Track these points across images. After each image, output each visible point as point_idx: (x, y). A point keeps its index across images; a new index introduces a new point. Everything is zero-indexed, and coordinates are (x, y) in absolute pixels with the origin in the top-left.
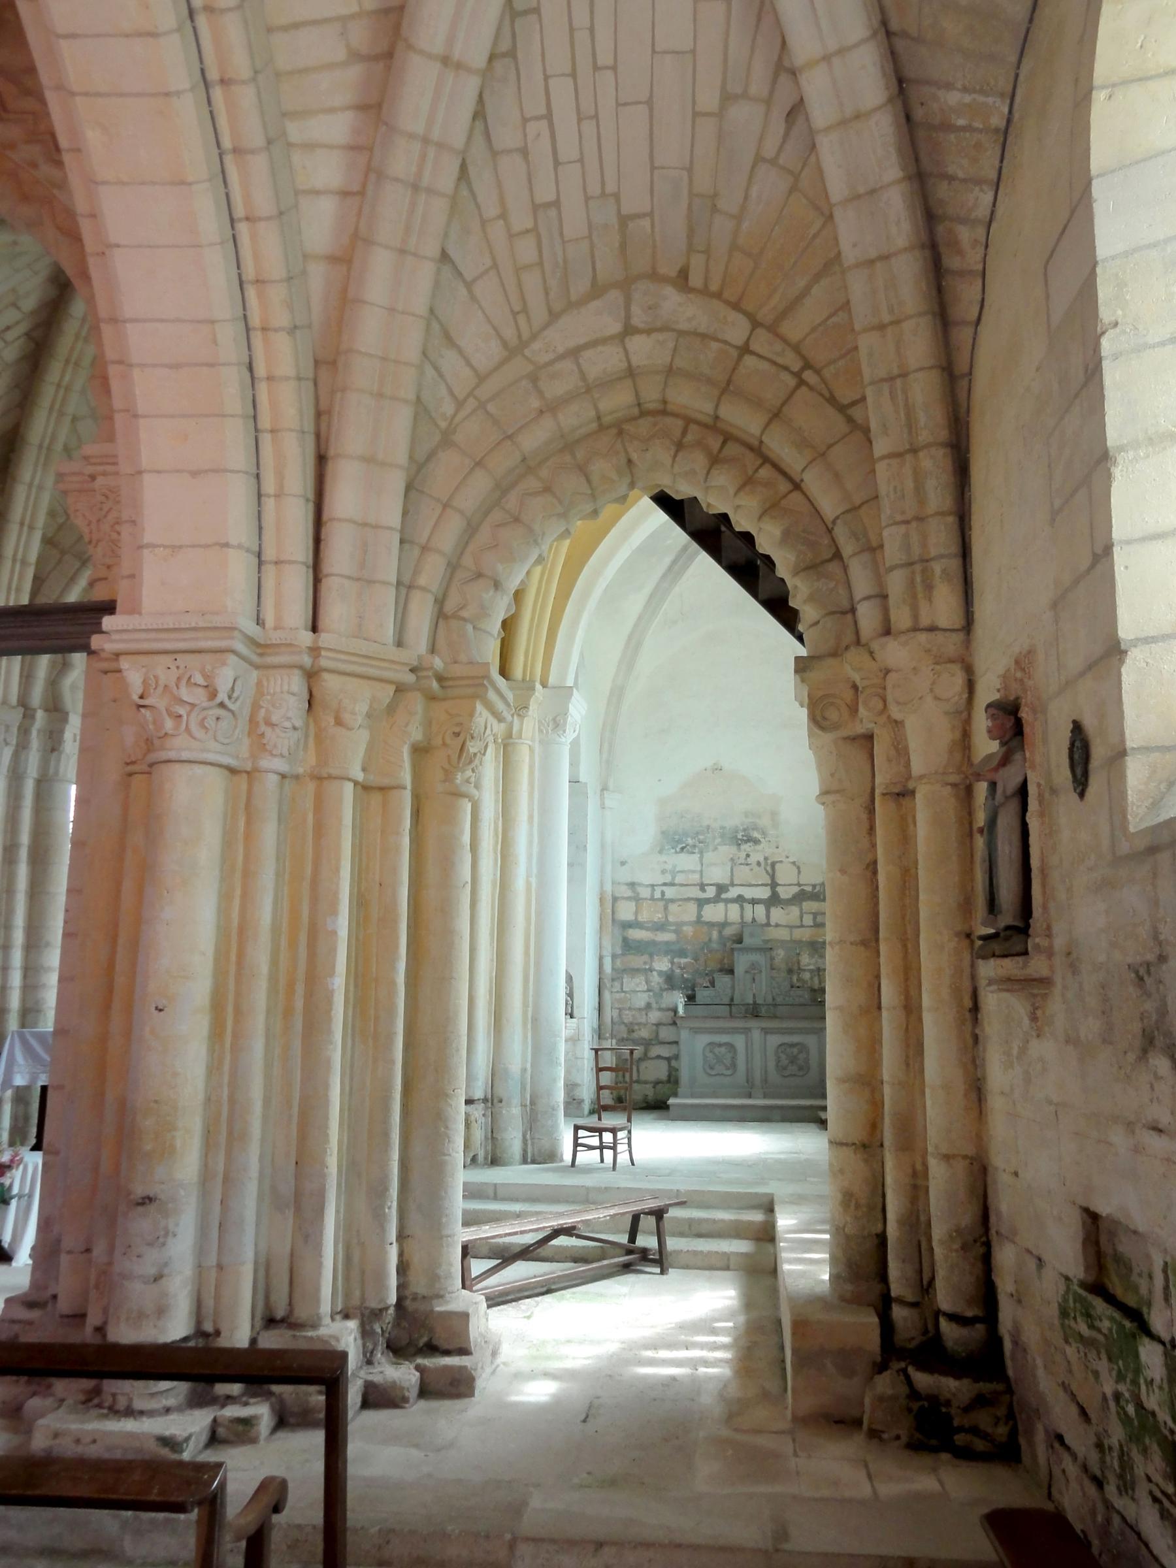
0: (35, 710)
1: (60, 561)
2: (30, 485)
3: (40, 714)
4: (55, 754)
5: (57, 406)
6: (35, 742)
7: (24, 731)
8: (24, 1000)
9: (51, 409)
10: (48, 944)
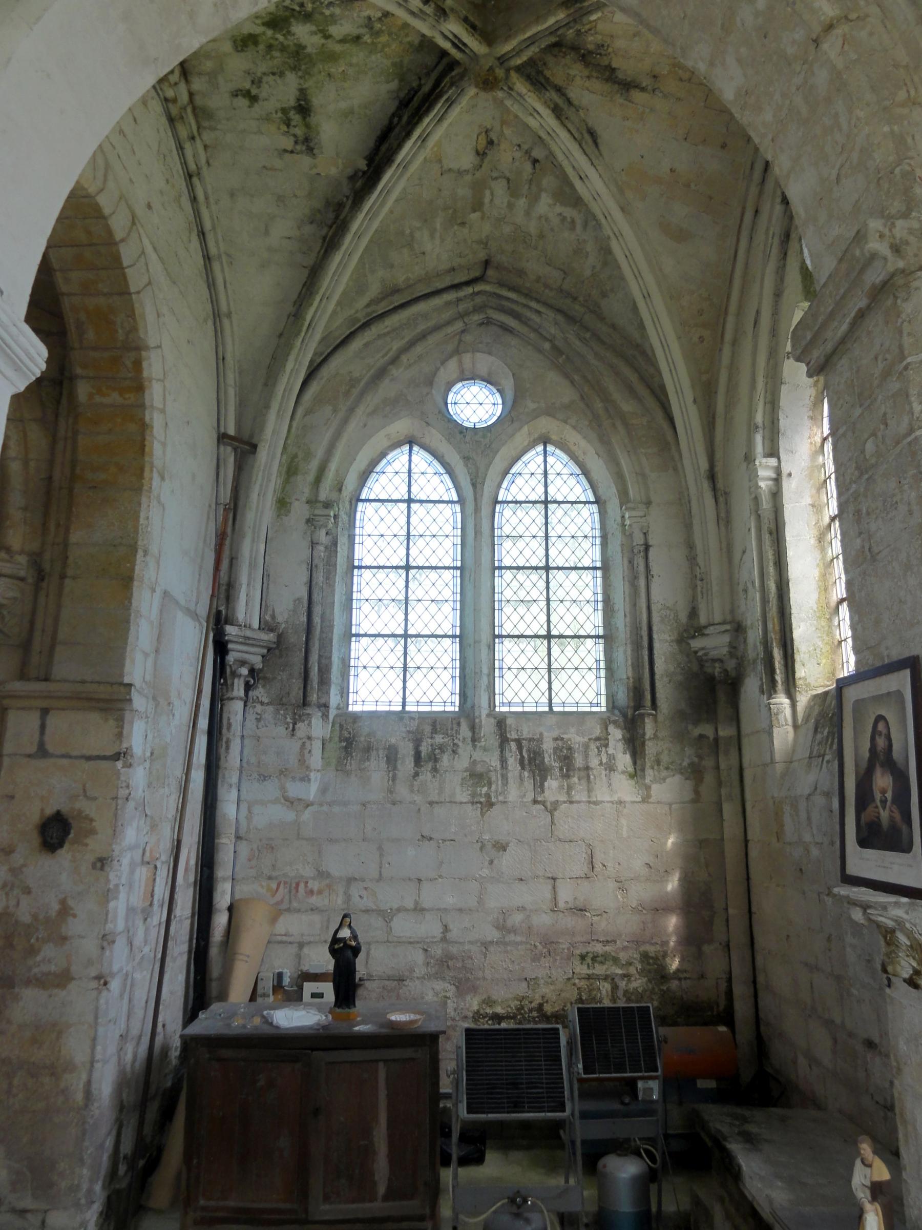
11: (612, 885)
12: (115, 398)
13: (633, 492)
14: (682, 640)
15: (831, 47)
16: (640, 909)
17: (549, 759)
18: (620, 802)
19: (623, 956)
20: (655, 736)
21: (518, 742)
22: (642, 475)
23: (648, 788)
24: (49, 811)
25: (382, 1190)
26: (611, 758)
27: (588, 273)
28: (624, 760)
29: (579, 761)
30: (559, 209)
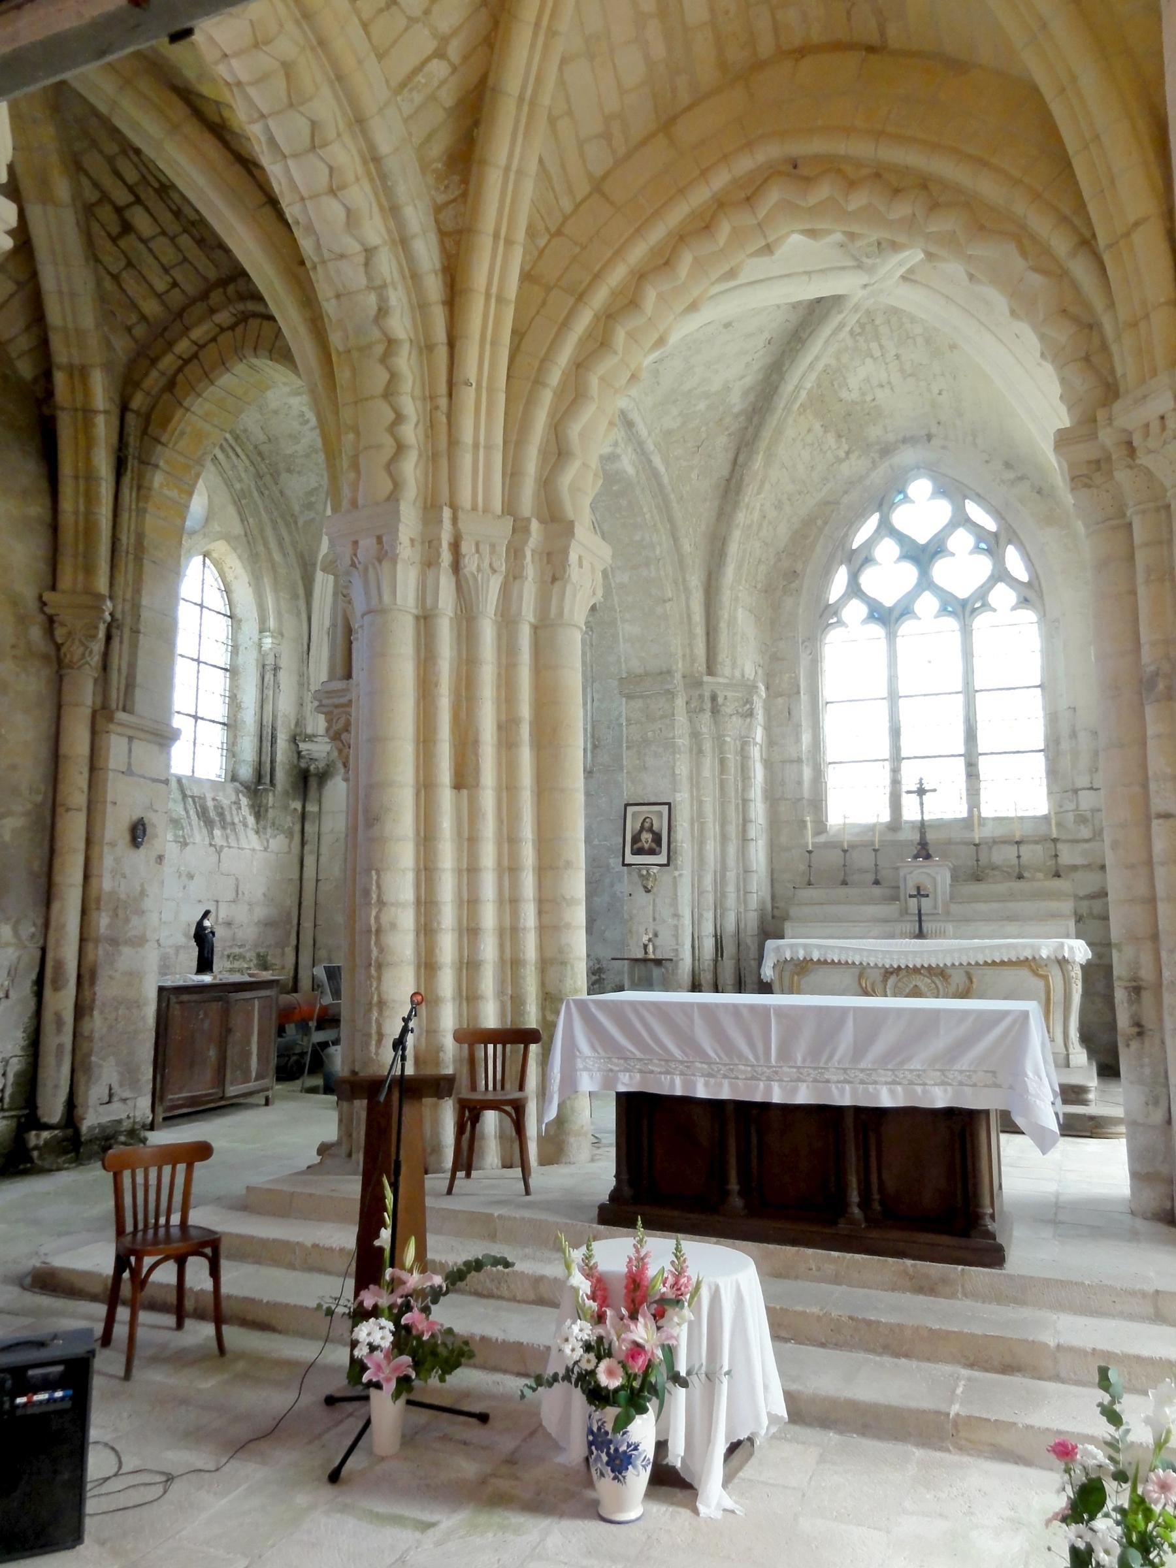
0: (528, 520)
1: (544, 303)
2: (507, 169)
3: (535, 526)
4: (558, 584)
5: (545, 23)
6: (530, 571)
7: (515, 553)
8: (541, 948)
9: (537, 25)
10: (568, 864)
11: (246, 907)
12: (174, 494)
13: (272, 623)
14: (294, 740)
15: (668, 605)
16: (258, 923)
17: (212, 814)
18: (254, 850)
19: (248, 955)
20: (273, 807)
21: (193, 797)
22: (279, 614)
23: (268, 842)
24: (135, 817)
25: (254, 1075)
26: (245, 818)
27: (289, 452)
28: (251, 820)
29: (228, 819)
30: (304, 409)
